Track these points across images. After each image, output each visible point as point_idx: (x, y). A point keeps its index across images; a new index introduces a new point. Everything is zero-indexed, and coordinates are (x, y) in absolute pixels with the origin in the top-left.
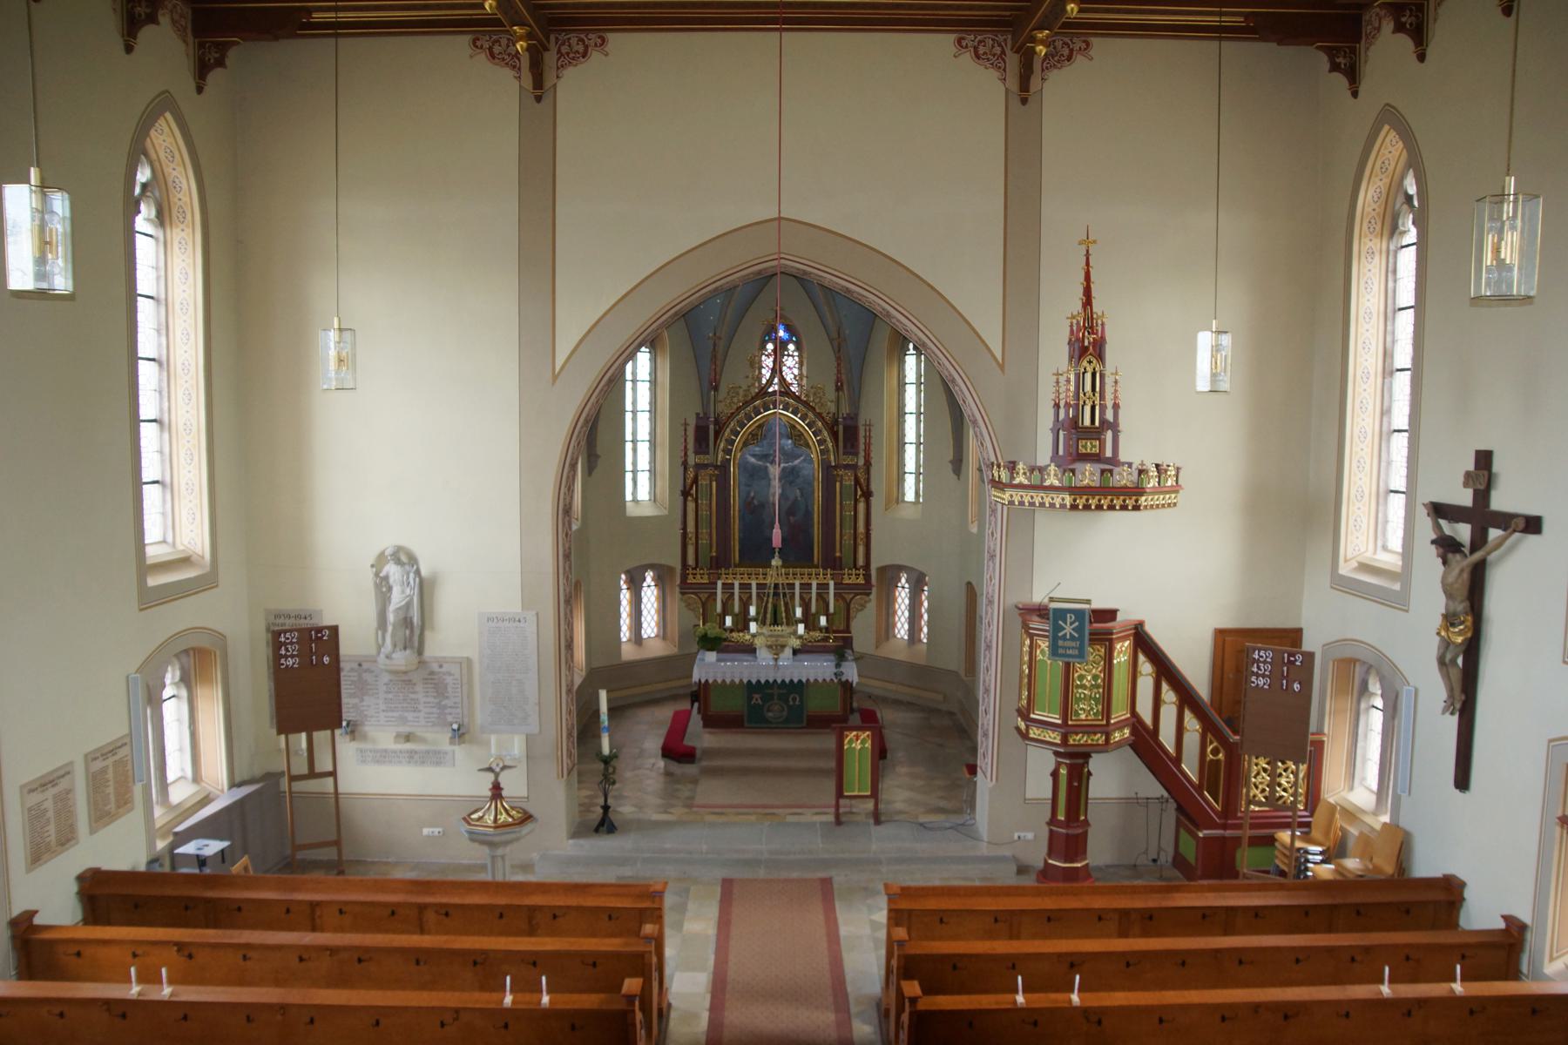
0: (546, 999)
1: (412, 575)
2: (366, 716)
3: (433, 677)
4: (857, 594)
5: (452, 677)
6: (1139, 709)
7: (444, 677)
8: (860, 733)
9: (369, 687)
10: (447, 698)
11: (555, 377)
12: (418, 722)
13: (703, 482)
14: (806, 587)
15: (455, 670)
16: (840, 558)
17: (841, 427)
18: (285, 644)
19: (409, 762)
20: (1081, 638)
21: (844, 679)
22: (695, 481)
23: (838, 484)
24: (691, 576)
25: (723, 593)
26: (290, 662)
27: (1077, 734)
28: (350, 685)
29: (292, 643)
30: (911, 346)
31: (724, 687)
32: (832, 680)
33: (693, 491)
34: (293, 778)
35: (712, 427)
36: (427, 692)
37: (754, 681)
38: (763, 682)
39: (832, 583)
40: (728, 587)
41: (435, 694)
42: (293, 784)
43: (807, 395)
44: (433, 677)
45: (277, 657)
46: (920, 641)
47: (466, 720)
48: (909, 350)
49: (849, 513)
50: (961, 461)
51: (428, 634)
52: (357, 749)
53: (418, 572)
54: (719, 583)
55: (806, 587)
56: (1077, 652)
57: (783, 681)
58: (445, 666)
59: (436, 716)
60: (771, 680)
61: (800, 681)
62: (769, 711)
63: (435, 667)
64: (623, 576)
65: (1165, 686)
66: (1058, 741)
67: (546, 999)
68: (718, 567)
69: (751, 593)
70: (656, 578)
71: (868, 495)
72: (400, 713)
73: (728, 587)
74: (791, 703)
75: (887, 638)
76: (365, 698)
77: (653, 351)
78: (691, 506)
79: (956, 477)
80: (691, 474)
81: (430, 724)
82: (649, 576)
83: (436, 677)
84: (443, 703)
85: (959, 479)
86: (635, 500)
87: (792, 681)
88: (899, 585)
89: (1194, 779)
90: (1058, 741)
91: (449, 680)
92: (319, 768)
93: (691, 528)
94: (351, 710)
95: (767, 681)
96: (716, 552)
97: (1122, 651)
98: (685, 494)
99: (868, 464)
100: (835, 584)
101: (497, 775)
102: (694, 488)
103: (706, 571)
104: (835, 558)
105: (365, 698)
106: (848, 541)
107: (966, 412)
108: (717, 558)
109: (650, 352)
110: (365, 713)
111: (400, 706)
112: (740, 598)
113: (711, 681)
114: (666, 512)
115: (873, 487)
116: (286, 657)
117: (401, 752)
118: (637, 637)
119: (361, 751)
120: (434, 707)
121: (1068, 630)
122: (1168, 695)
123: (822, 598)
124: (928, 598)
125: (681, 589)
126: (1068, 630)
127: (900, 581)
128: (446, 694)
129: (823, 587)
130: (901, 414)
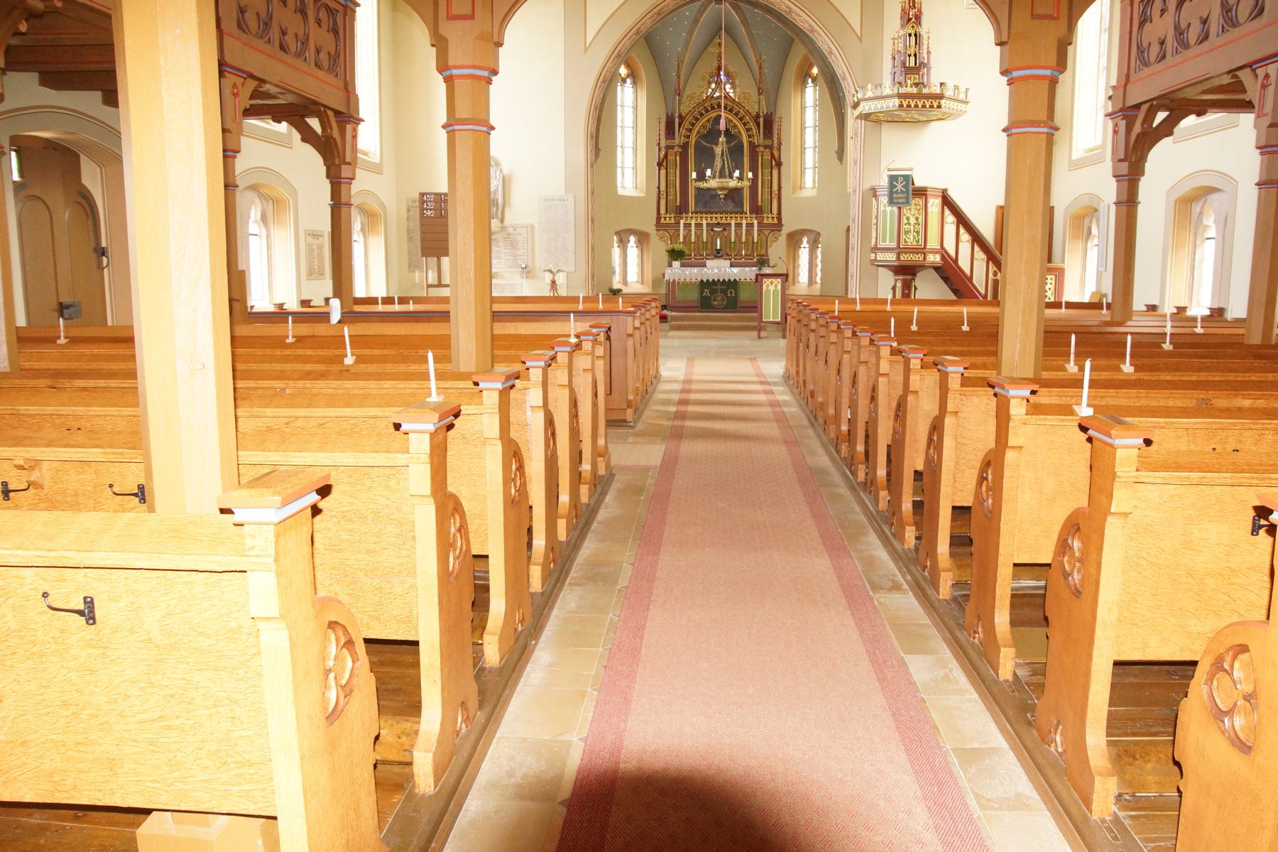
0: (601, 306)
1: (498, 172)
4: (772, 231)
6: (945, 245)
8: (773, 280)
10: (518, 250)
11: (586, 49)
13: (671, 158)
14: (739, 225)
15: (523, 231)
17: (762, 120)
18: (426, 202)
20: (907, 192)
22: (666, 156)
23: (760, 158)
26: (429, 213)
27: (906, 253)
29: (430, 202)
30: (810, 80)
31: (686, 285)
33: (664, 164)
34: (429, 286)
35: (677, 120)
40: (687, 226)
42: (429, 289)
43: (739, 99)
45: (422, 209)
46: (816, 282)
47: (530, 264)
49: (767, 178)
50: (843, 151)
51: (507, 210)
53: (501, 171)
54: (682, 222)
55: (739, 225)
56: (904, 200)
57: (724, 280)
62: (714, 300)
63: (511, 230)
64: (615, 238)
65: (962, 230)
66: (894, 259)
67: (601, 306)
68: (681, 213)
71: (779, 164)
73: (687, 226)
75: (794, 284)
78: (663, 172)
79: (839, 163)
80: (663, 153)
82: (632, 239)
87: (729, 280)
89: (983, 291)
90: (894, 259)
91: (520, 238)
92: (443, 283)
93: (663, 188)
97: (935, 204)
98: (660, 165)
99: (780, 144)
100: (758, 223)
101: (554, 275)
103: (673, 215)
104: (758, 206)
106: (767, 196)
107: (839, 72)
108: (680, 206)
112: (695, 233)
113: (677, 280)
114: (644, 195)
115: (783, 159)
116: (427, 210)
118: (625, 282)
121: (899, 187)
122: (965, 236)
123: (749, 232)
124: (822, 253)
126: (899, 187)
129: (750, 225)
130: (803, 128)
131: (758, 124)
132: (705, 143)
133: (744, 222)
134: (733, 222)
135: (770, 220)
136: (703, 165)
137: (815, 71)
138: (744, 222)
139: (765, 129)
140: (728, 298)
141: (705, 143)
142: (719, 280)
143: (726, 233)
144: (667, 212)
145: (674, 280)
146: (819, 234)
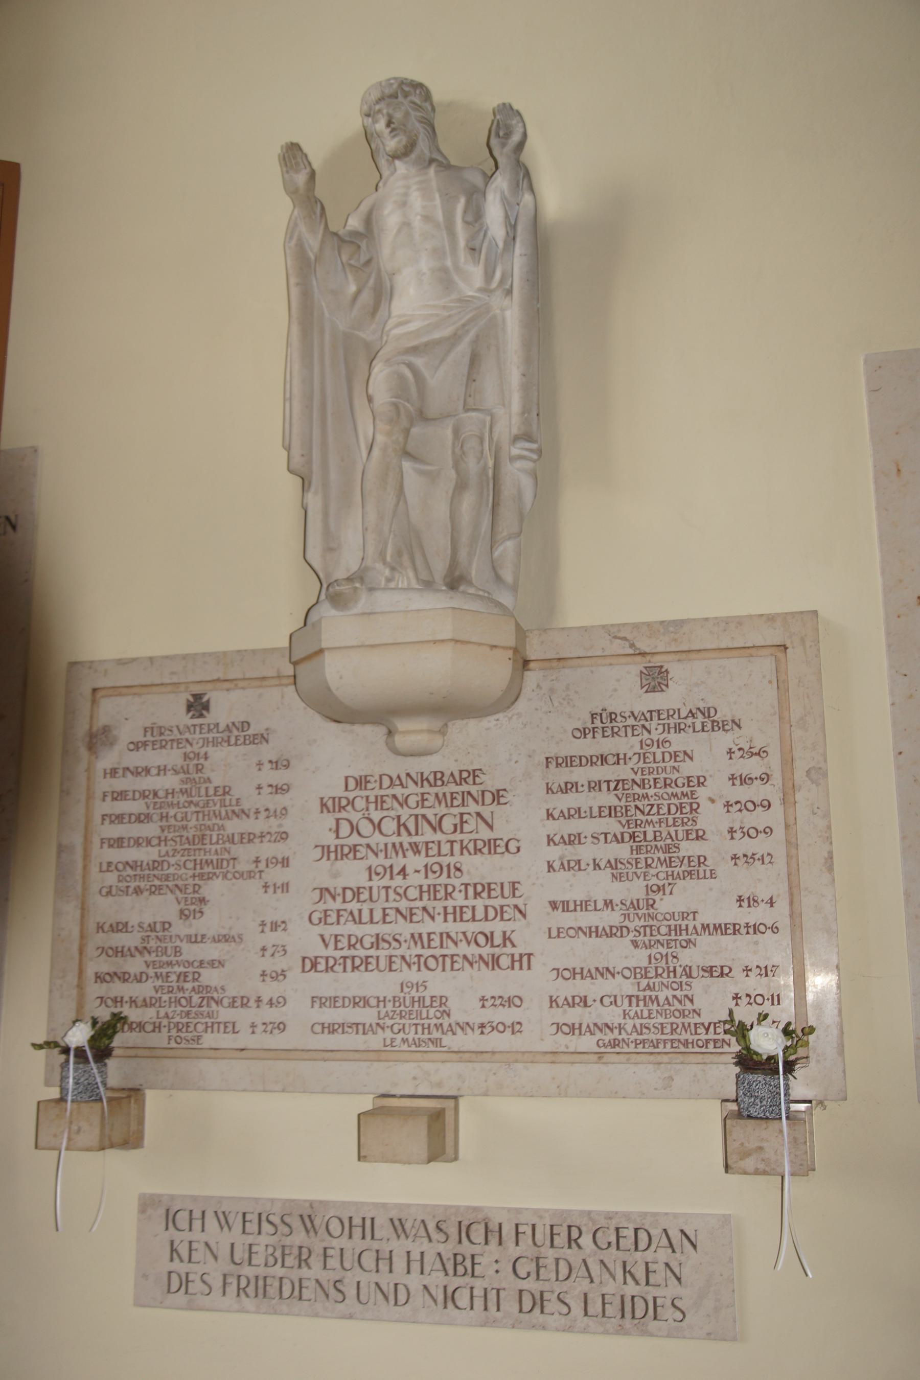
2: (209, 996)
3: (607, 745)
5: (724, 740)
7: (678, 742)
9: (234, 826)
12: (515, 1028)
19: (450, 1298)
28: (140, 819)
36: (574, 839)
41: (623, 851)
44: (607, 745)
52: (147, 1203)
58: (676, 670)
59: (629, 987)
72: (413, 975)
76: (215, 889)
81: (587, 1043)
83: (627, 745)
84: (665, 905)
94: (135, 965)
105: (215, 889)
110: (210, 977)
111: (404, 929)
117: (399, 1227)
119: (170, 1219)
120: (610, 933)
128: (688, 848)
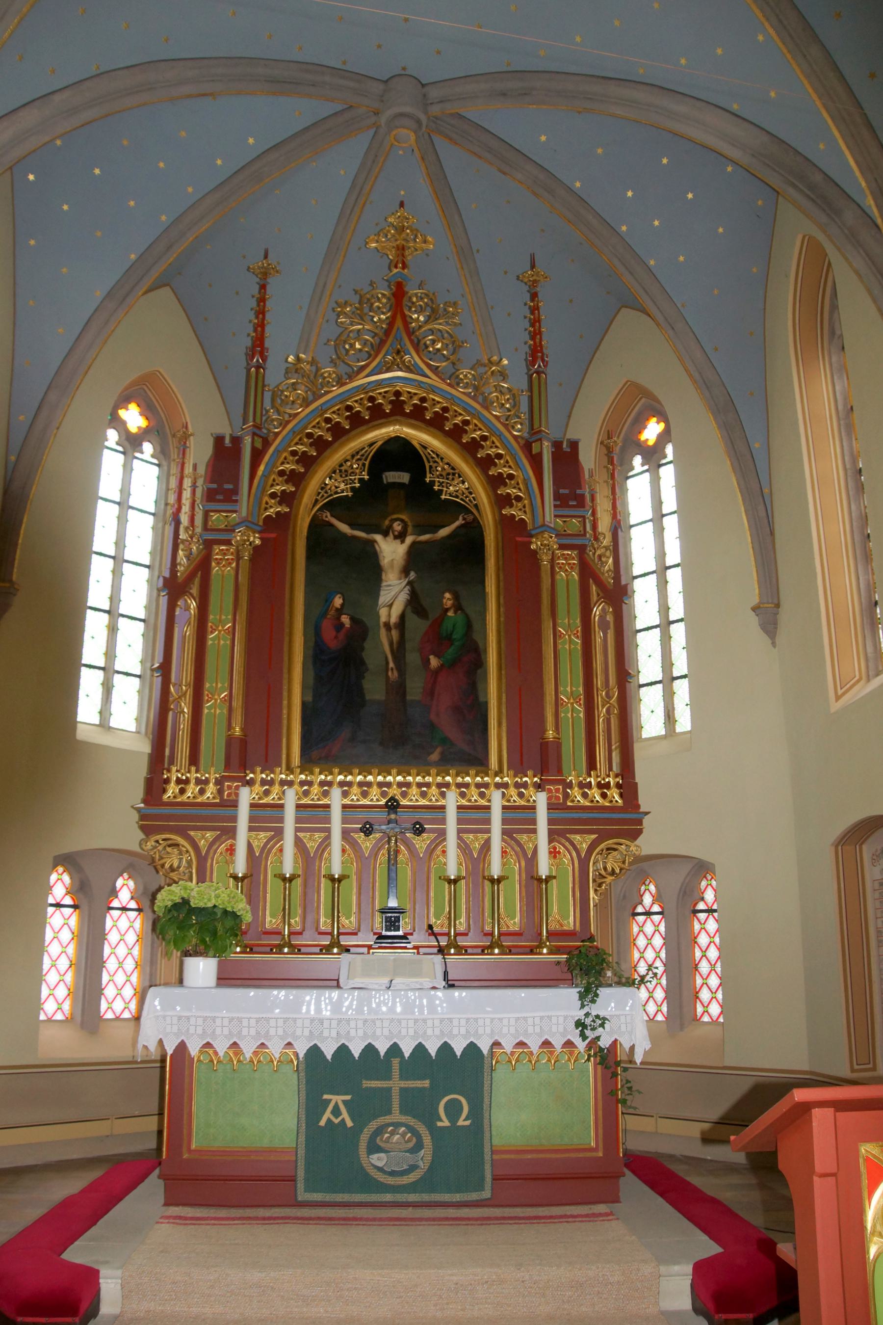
4: (603, 836)
16: (558, 744)
21: (605, 1043)
24: (172, 790)
25: (251, 829)
32: (569, 1044)
33: (195, 591)
37: (329, 1051)
38: (356, 1051)
39: (541, 800)
48: (632, 468)
54: (246, 797)
57: (420, 1049)
60: (382, 1048)
61: (472, 1049)
62: (374, 1148)
68: (244, 766)
69: (328, 830)
70: (141, 891)
74: (446, 1123)
77: (165, 463)
85: (774, 644)
86: (104, 724)
87: (446, 1048)
88: (640, 909)
95: (370, 1049)
96: (242, 729)
100: (551, 807)
102: (197, 581)
104: (544, 746)
108: (243, 742)
109: (158, 465)
112: (299, 843)
113: (194, 1049)
125: (143, 817)
127: (641, 903)
131: (536, 461)
132: (344, 528)
133: (497, 801)
134: (452, 801)
135: (595, 794)
136: (338, 601)
137: (652, 431)
138: (497, 801)
139: (558, 482)
140: (434, 1131)
141: (344, 528)
142: (395, 1049)
143: (421, 843)
144: (194, 760)
145: (182, 1047)
146: (702, 869)
